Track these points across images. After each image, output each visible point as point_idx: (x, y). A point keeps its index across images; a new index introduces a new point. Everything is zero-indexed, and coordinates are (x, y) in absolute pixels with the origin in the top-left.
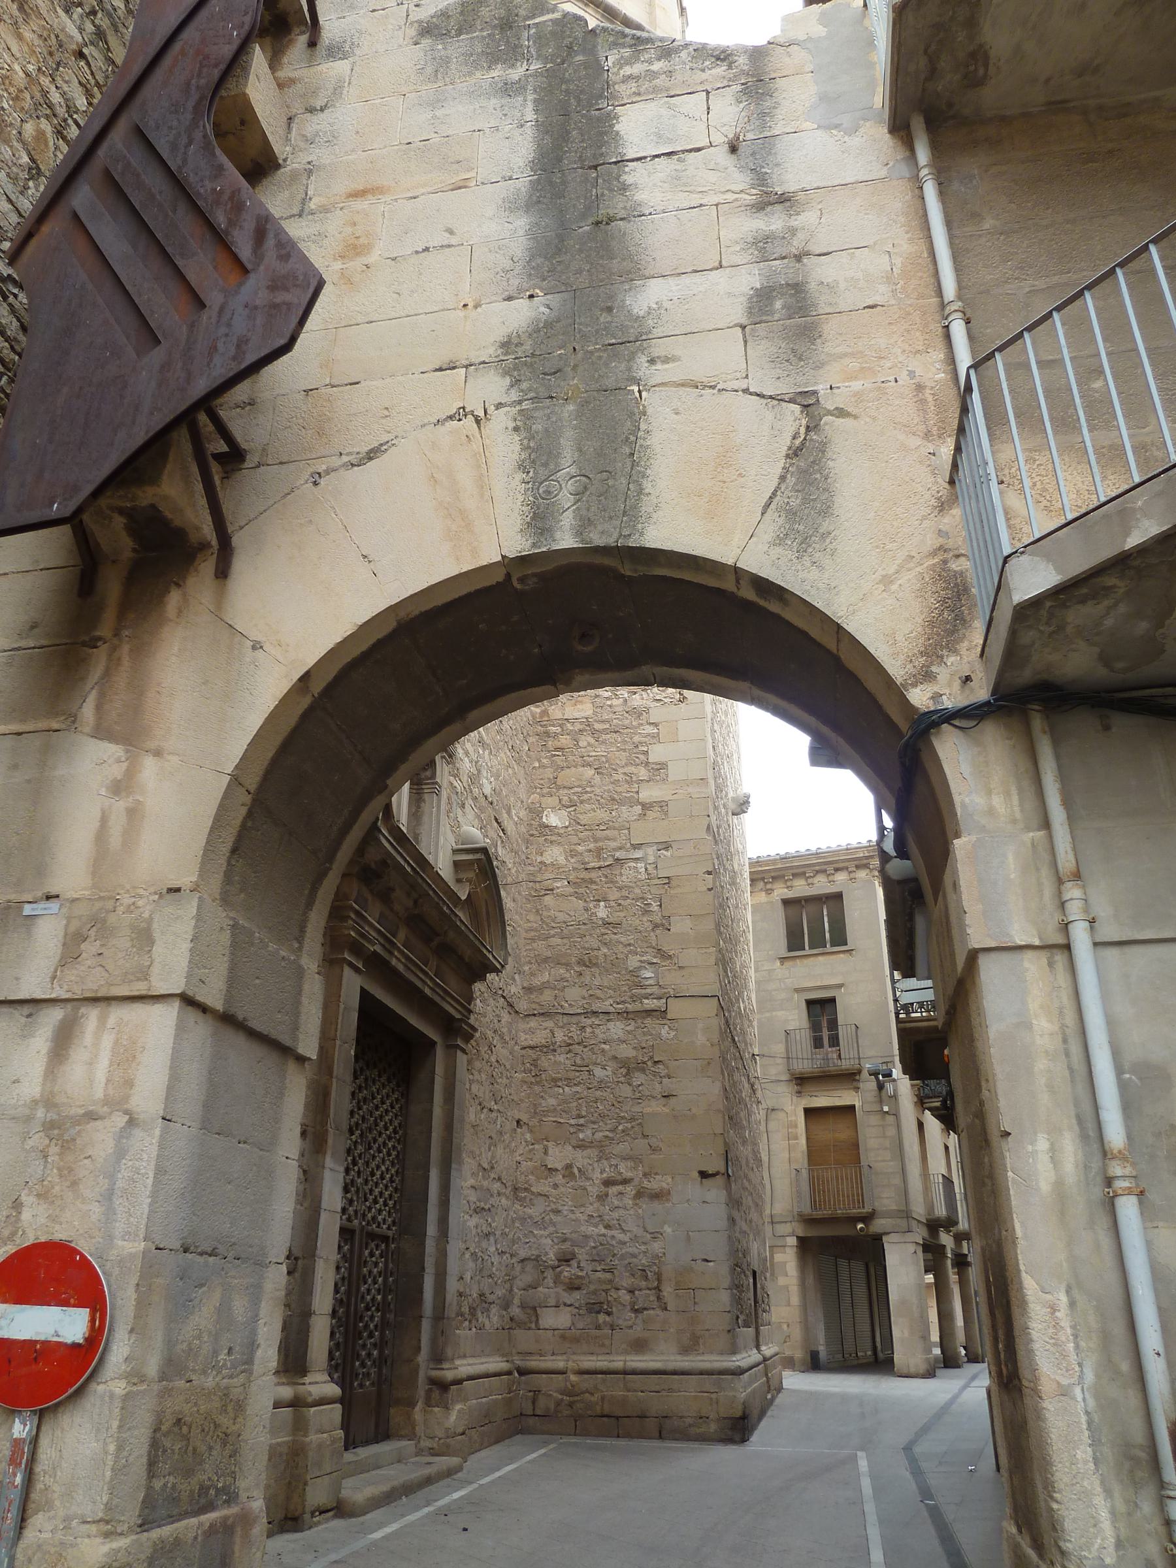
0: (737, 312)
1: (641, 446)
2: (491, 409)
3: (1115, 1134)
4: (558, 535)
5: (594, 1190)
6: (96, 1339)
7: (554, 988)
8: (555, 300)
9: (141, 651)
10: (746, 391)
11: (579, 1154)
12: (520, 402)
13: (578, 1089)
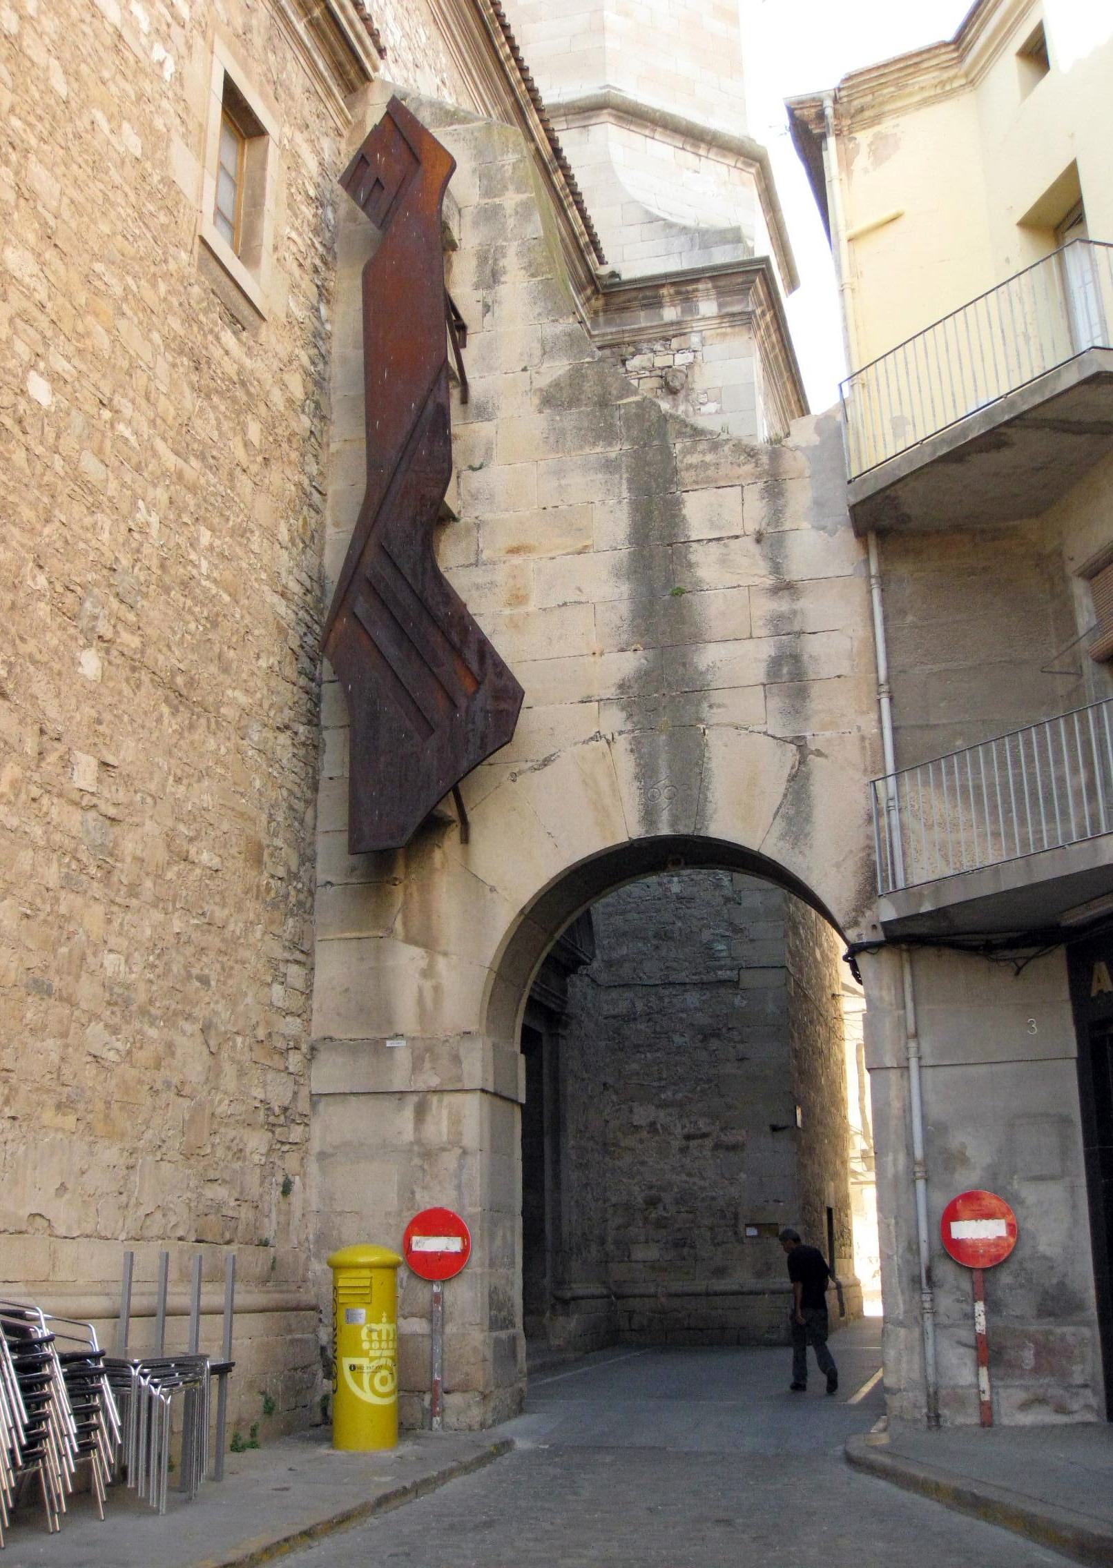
0: (757, 672)
2: (616, 735)
3: (919, 1153)
4: (660, 825)
5: (676, 1144)
6: (465, 1251)
7: (634, 960)
8: (650, 653)
9: (425, 888)
10: (765, 733)
11: (662, 1113)
12: (633, 731)
13: (658, 1054)
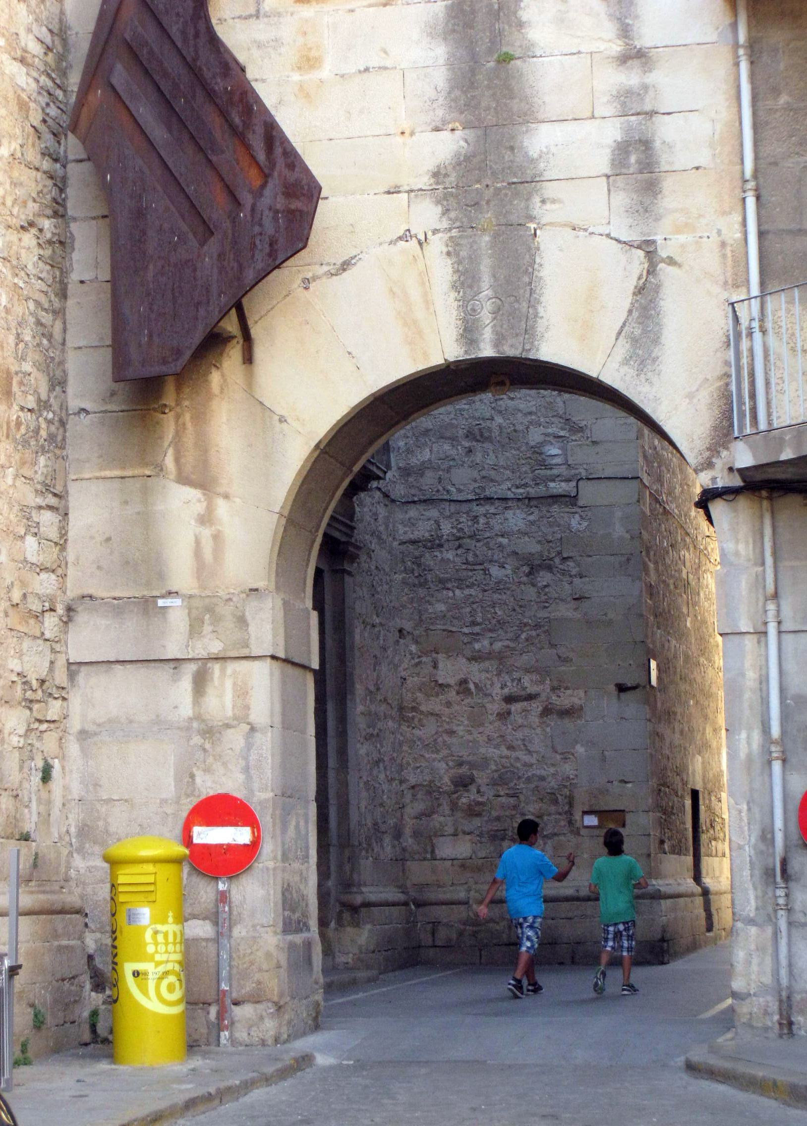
0: (602, 162)
1: (537, 277)
2: (429, 234)
3: (776, 731)
4: (482, 345)
5: (495, 707)
6: (255, 844)
7: (437, 469)
8: (470, 134)
9: (201, 418)
10: (608, 236)
11: (475, 667)
12: (450, 230)
13: (472, 591)
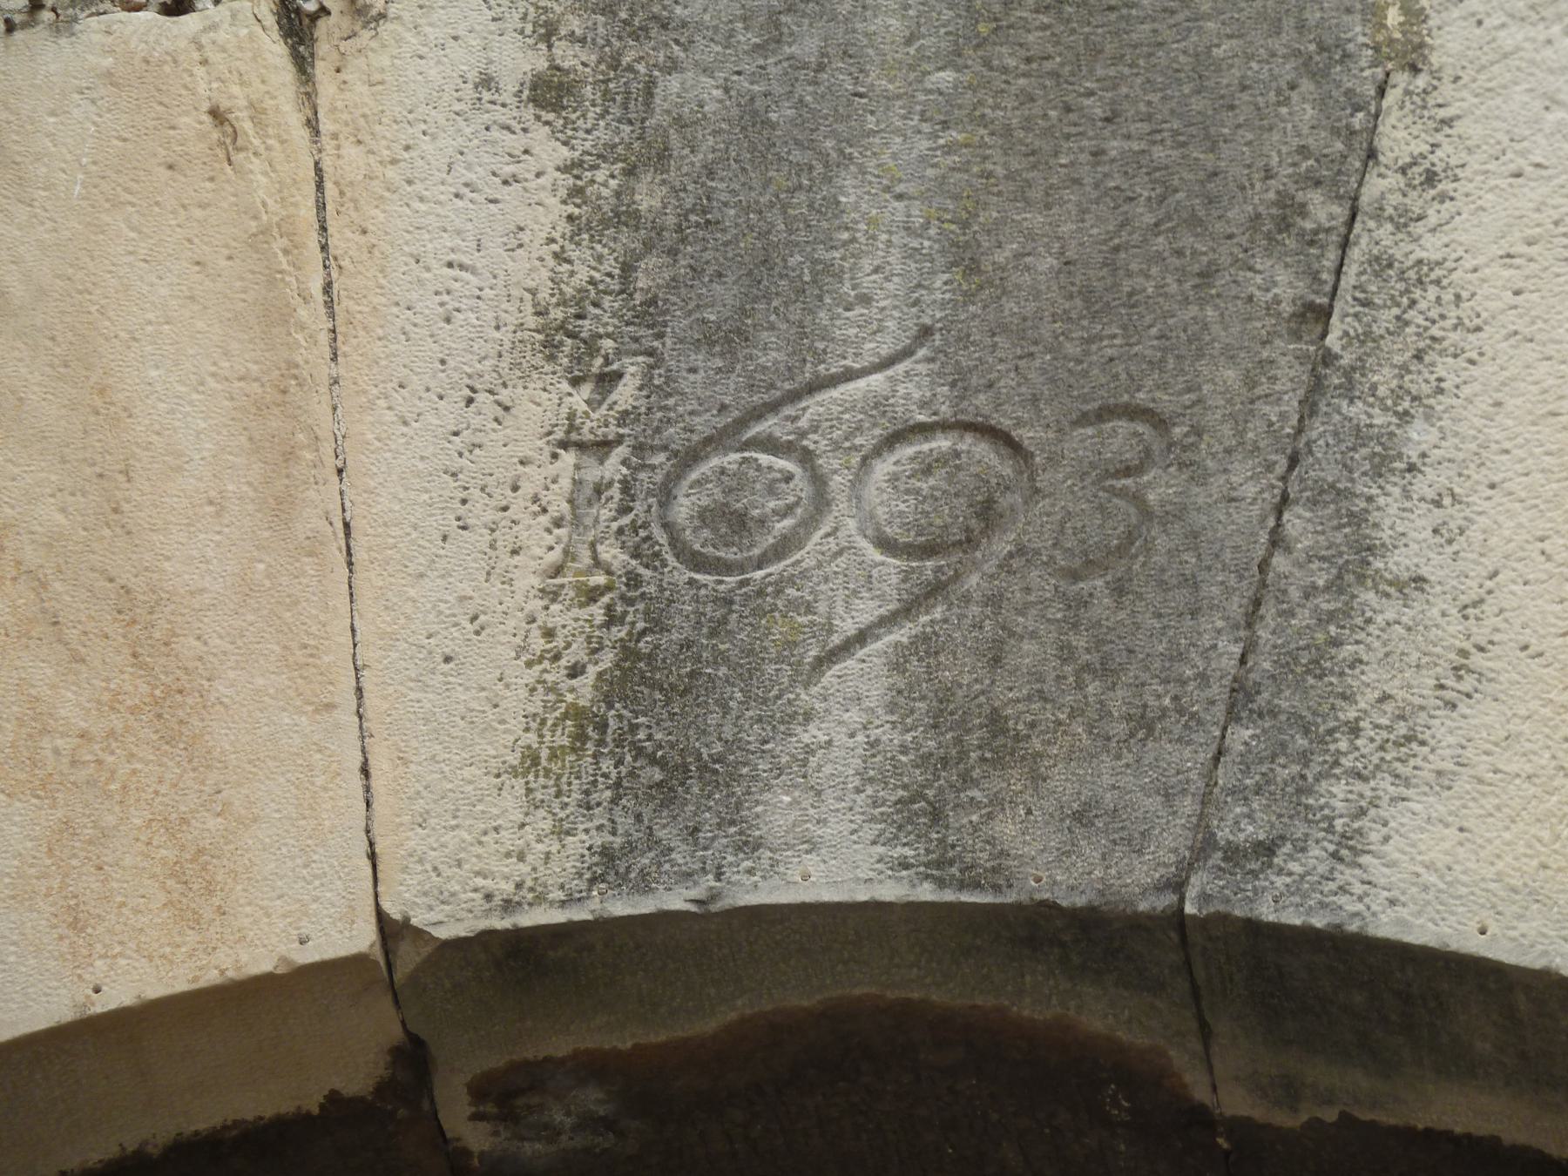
1: (1381, 264)
